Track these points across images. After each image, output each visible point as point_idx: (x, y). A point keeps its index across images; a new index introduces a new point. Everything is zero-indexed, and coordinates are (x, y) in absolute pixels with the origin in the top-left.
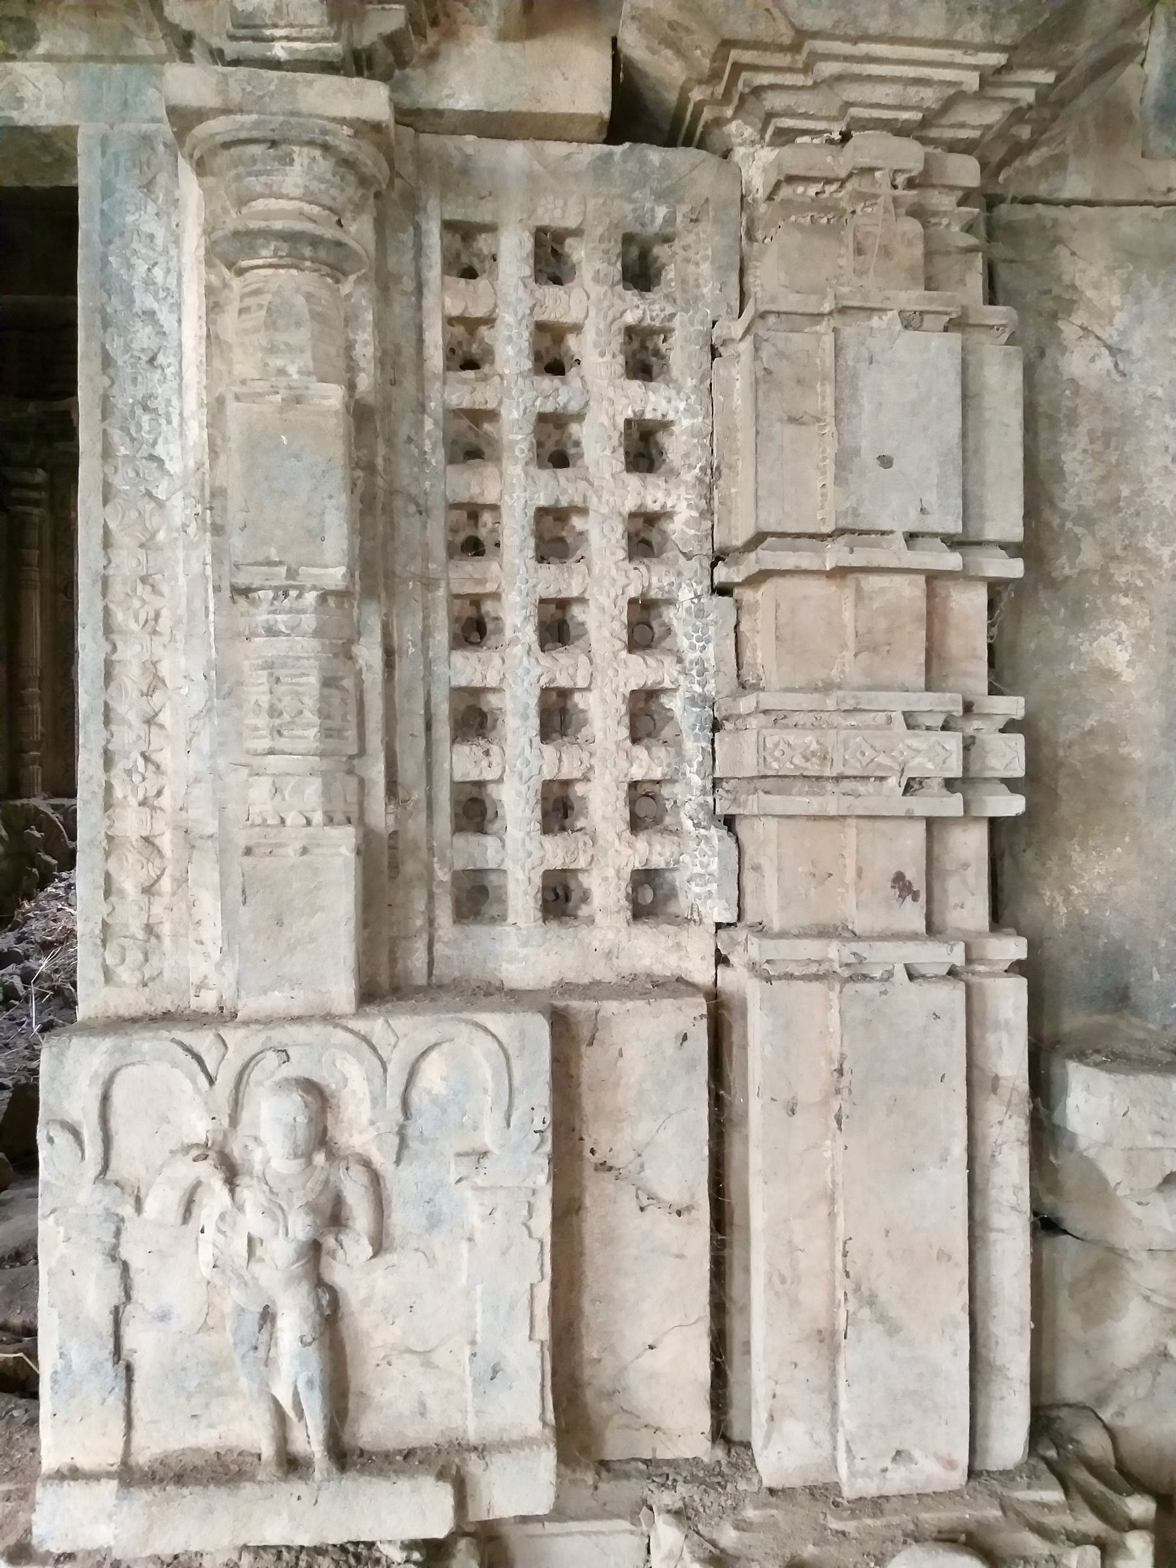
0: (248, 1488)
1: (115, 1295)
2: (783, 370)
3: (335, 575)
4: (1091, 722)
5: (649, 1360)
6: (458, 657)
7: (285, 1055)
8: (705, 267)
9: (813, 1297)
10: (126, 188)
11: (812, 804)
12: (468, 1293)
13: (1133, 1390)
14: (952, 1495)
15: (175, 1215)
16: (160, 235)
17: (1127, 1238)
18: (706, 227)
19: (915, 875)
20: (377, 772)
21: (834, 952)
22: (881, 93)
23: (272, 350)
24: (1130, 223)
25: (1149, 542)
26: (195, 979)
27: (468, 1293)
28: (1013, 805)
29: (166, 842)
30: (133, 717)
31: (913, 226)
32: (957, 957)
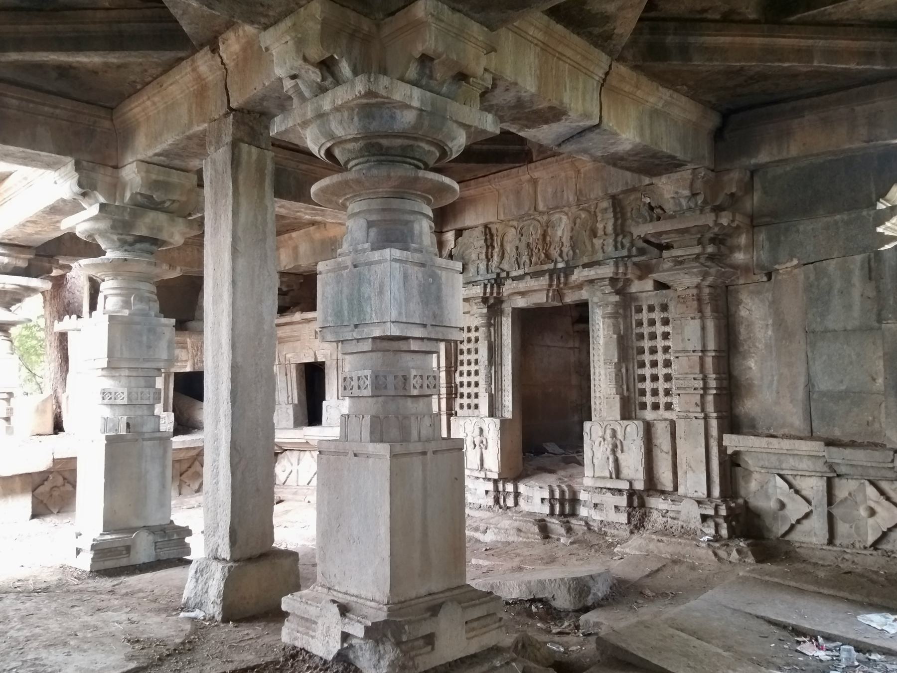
3: (616, 360)
19: (699, 403)
20: (625, 387)
24: (752, 287)
25: (757, 344)
28: (702, 392)
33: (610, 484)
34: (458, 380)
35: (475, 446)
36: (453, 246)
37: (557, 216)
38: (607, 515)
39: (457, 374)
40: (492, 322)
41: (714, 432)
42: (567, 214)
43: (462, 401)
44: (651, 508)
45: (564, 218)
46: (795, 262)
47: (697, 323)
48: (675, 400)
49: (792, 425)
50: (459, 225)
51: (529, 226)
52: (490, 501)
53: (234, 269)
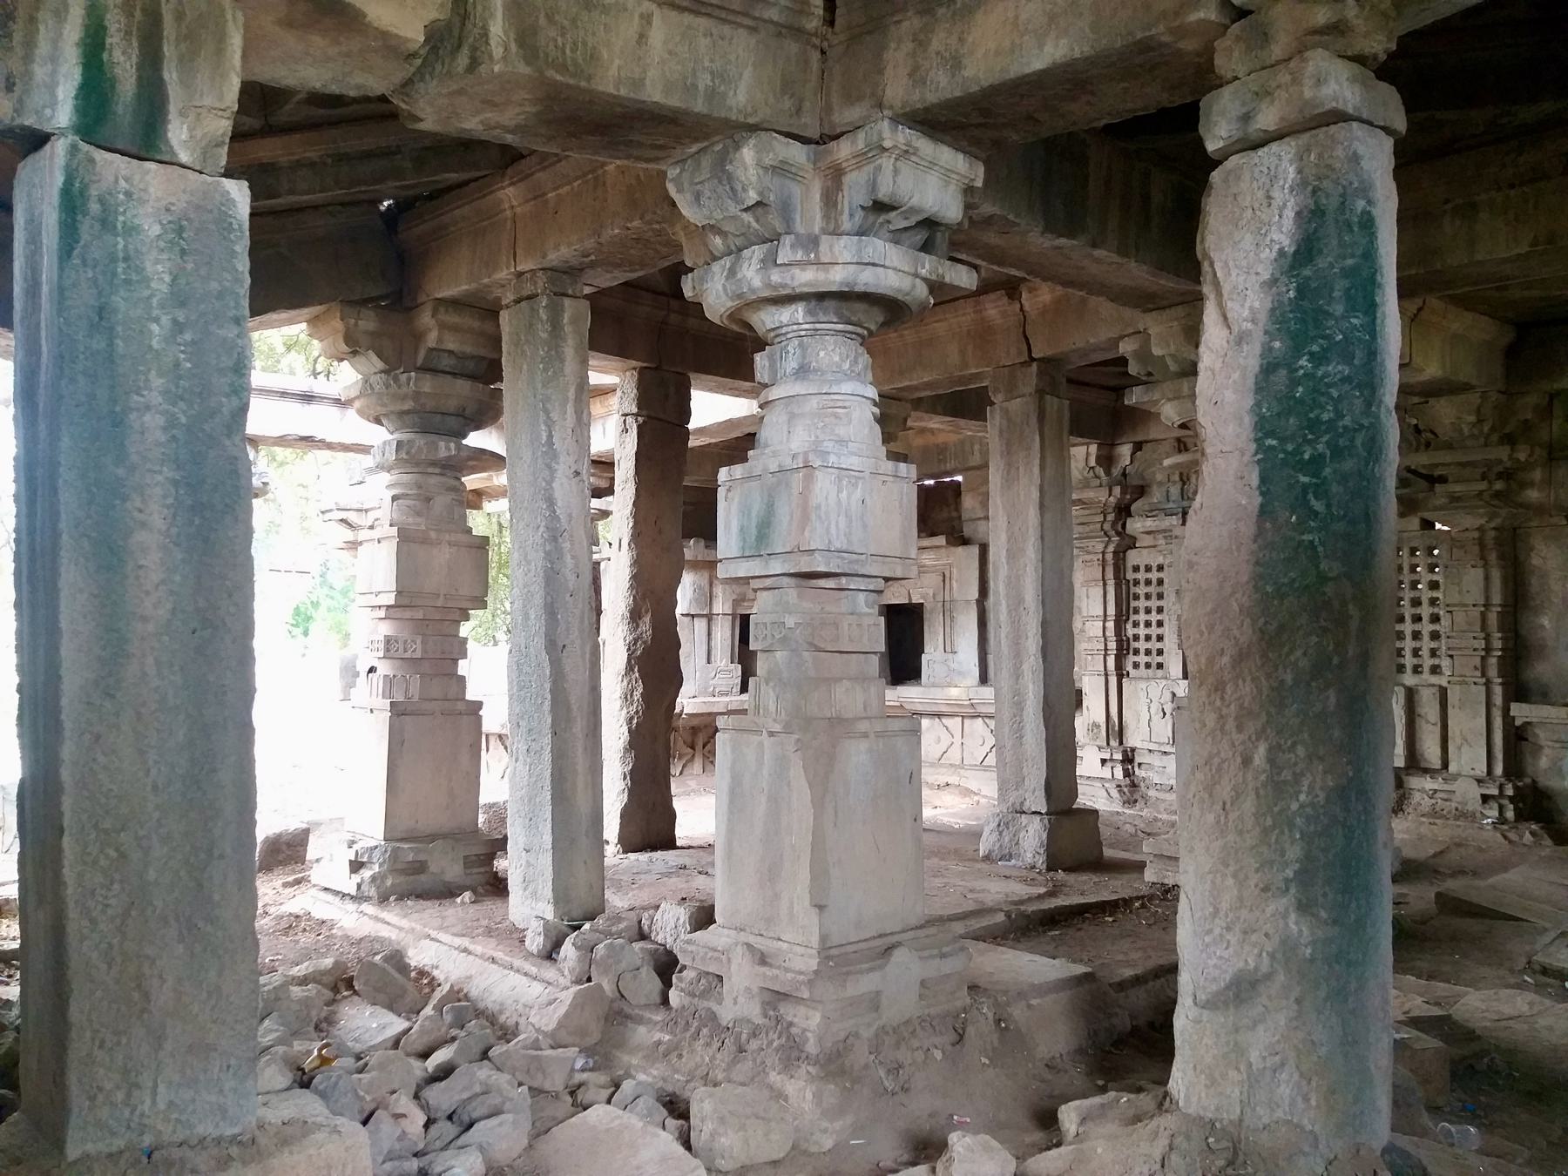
19: (1479, 665)
28: (1483, 653)
34: (1130, 631)
39: (1129, 626)
41: (1498, 700)
43: (1136, 659)
47: (1480, 572)
48: (1445, 663)
50: (1139, 438)
53: (1042, 525)
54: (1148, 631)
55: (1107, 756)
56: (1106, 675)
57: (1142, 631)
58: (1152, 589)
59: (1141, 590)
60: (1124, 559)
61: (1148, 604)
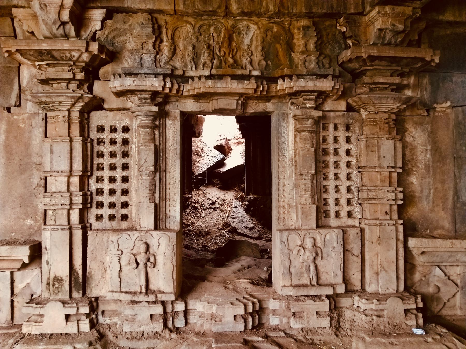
0: (308, 288)
1: (290, 264)
2: (370, 145)
3: (313, 172)
4: (410, 190)
5: (353, 276)
6: (324, 182)
7: (309, 233)
8: (357, 128)
9: (375, 268)
10: (281, 120)
11: (375, 202)
12: (332, 265)
13: (417, 285)
14: (395, 294)
15: (297, 254)
16: (285, 126)
17: (416, 263)
18: (357, 123)
19: (388, 212)
20: (316, 197)
21: (378, 222)
22: (383, 109)
23: (305, 144)
24: (415, 119)
25: (418, 164)
26: (290, 224)
27: (332, 265)
29: (286, 206)
30: (282, 190)
31: (387, 125)
32: (394, 222)
33: (313, 292)
34: (93, 186)
35: (138, 264)
36: (98, 26)
37: (245, 23)
38: (308, 322)
39: (92, 181)
40: (157, 123)
41: (401, 237)
42: (256, 24)
43: (100, 212)
44: (341, 307)
45: (253, 28)
46: (449, 104)
48: (357, 211)
49: (443, 228)
51: (210, 26)
52: (158, 326)
54: (112, 186)
55: (72, 311)
56: (71, 229)
57: (106, 186)
58: (118, 148)
59: (106, 149)
60: (88, 119)
61: (113, 161)
